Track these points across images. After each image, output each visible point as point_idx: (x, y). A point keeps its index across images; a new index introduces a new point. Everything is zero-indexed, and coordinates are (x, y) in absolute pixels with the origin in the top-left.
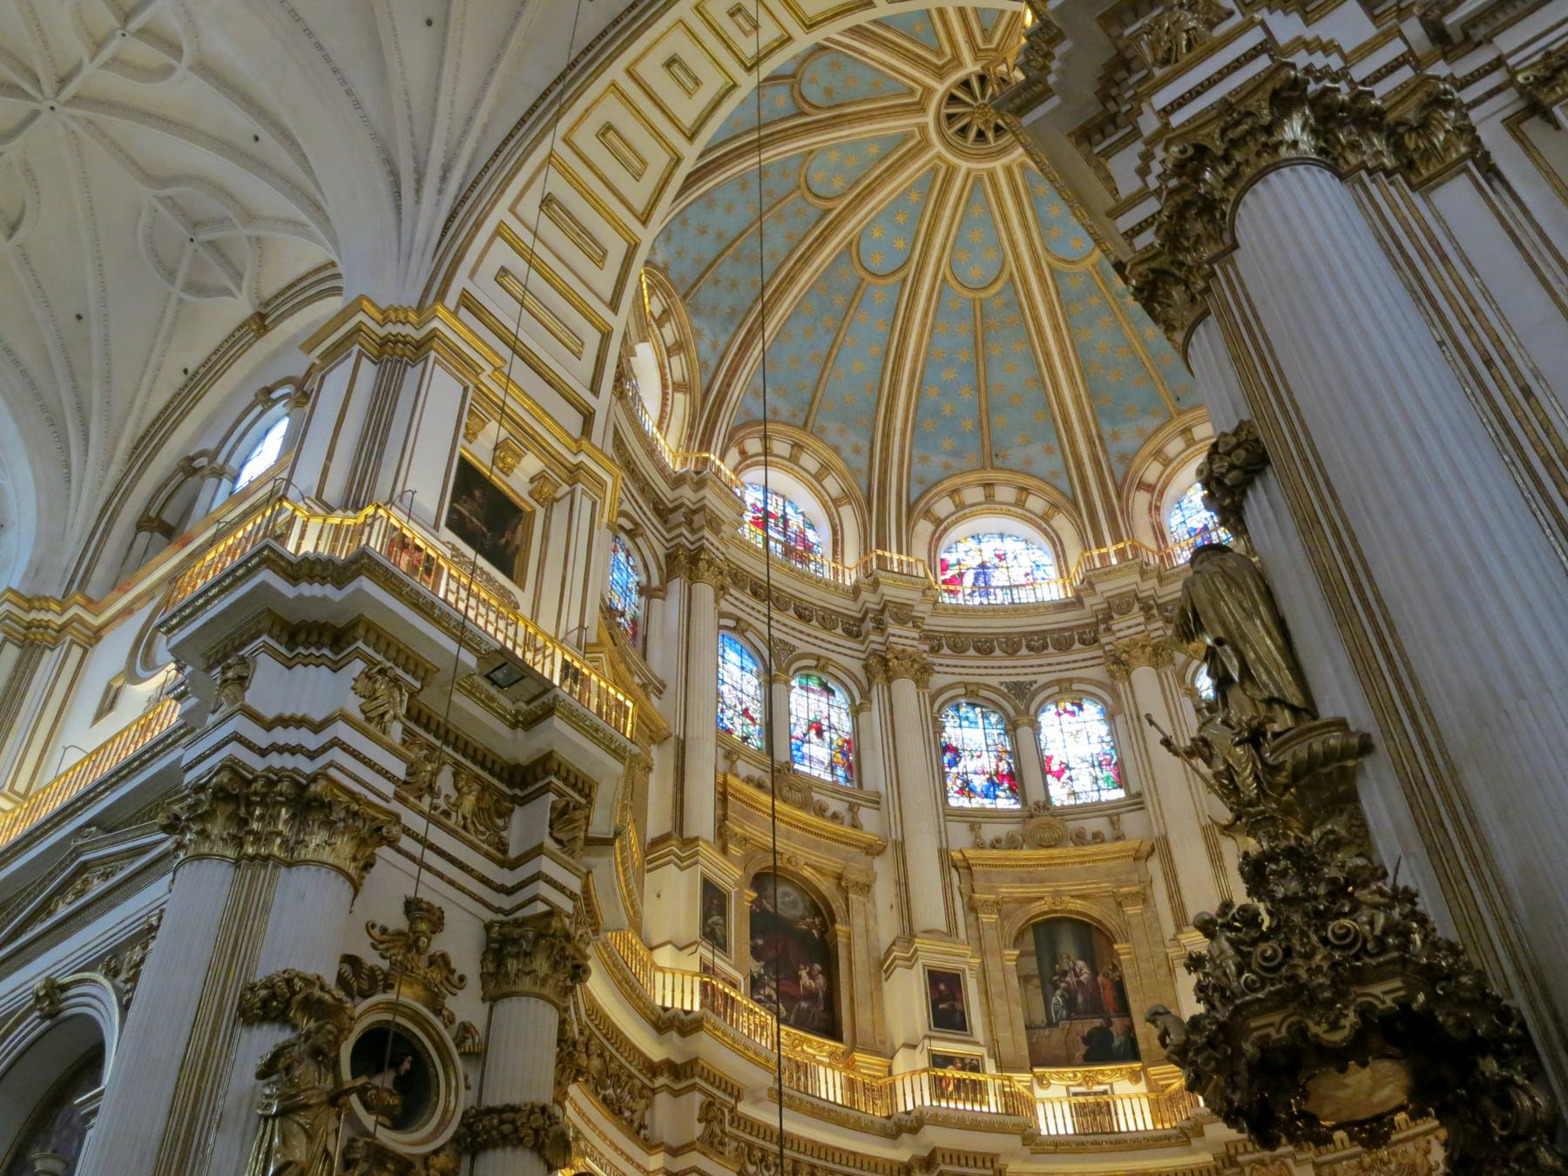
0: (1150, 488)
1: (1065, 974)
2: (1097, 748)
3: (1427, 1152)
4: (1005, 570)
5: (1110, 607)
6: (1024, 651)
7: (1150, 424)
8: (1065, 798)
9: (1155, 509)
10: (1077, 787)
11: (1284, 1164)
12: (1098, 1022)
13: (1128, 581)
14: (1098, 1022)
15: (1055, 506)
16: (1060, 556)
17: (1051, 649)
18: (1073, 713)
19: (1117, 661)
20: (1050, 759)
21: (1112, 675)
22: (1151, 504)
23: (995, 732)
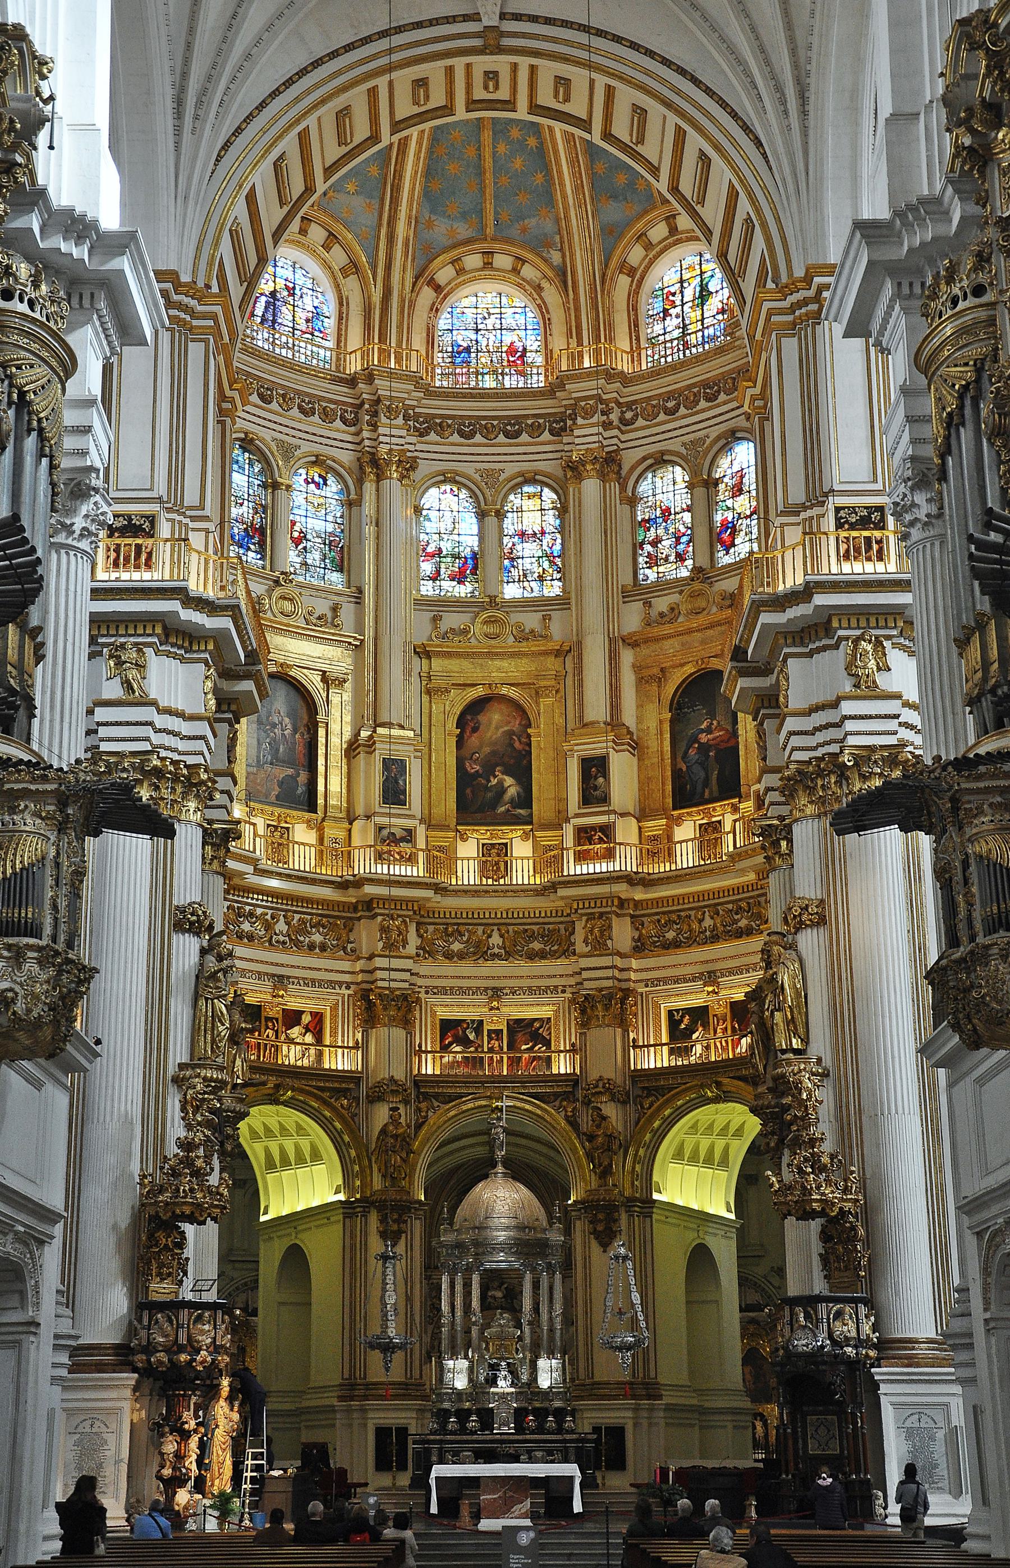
0: (438, 288)
1: (274, 726)
2: (330, 528)
3: (490, 936)
4: (291, 308)
5: (378, 401)
6: (295, 412)
7: (463, 231)
8: (298, 566)
9: (435, 310)
10: (309, 562)
11: (404, 921)
12: (290, 771)
13: (401, 389)
14: (290, 771)
15: (353, 267)
16: (342, 318)
17: (316, 418)
18: (318, 485)
19: (375, 461)
20: (294, 523)
21: (361, 468)
22: (434, 304)
23: (257, 482)
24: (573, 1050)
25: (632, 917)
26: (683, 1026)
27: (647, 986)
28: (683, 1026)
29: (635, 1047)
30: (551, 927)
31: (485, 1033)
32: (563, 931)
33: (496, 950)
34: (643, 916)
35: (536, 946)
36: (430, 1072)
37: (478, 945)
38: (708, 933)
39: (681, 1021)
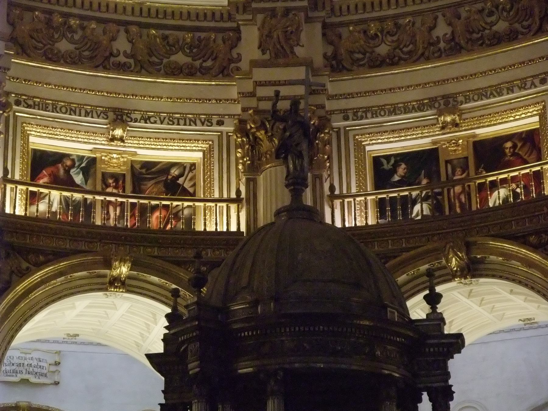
3: (113, 39)
24: (238, 200)
25: (325, 26)
26: (396, 178)
27: (346, 118)
28: (396, 178)
29: (333, 197)
30: (203, 35)
31: (99, 176)
32: (220, 41)
33: (122, 59)
34: (342, 24)
35: (180, 58)
36: (20, 211)
37: (95, 46)
38: (442, 45)
39: (394, 171)
